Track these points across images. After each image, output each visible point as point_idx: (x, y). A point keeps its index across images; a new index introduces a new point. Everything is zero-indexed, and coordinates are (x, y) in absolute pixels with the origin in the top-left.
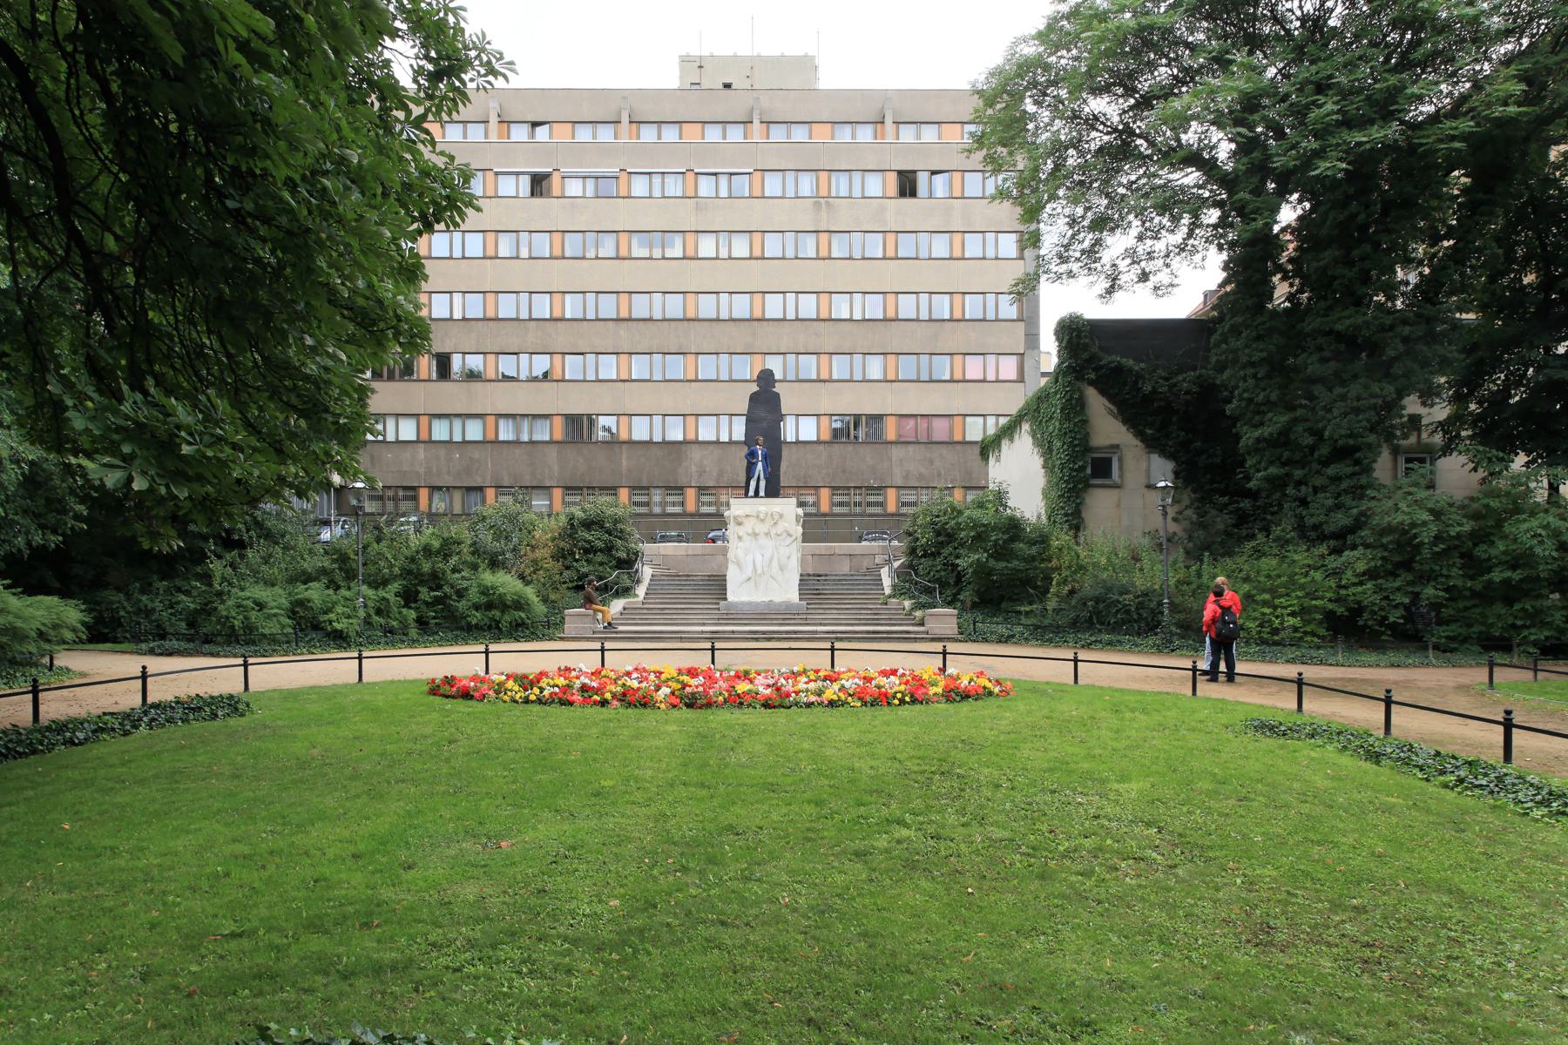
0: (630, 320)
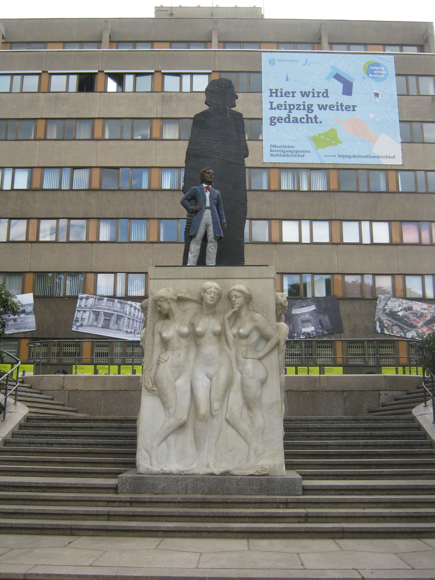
0: (101, 190)
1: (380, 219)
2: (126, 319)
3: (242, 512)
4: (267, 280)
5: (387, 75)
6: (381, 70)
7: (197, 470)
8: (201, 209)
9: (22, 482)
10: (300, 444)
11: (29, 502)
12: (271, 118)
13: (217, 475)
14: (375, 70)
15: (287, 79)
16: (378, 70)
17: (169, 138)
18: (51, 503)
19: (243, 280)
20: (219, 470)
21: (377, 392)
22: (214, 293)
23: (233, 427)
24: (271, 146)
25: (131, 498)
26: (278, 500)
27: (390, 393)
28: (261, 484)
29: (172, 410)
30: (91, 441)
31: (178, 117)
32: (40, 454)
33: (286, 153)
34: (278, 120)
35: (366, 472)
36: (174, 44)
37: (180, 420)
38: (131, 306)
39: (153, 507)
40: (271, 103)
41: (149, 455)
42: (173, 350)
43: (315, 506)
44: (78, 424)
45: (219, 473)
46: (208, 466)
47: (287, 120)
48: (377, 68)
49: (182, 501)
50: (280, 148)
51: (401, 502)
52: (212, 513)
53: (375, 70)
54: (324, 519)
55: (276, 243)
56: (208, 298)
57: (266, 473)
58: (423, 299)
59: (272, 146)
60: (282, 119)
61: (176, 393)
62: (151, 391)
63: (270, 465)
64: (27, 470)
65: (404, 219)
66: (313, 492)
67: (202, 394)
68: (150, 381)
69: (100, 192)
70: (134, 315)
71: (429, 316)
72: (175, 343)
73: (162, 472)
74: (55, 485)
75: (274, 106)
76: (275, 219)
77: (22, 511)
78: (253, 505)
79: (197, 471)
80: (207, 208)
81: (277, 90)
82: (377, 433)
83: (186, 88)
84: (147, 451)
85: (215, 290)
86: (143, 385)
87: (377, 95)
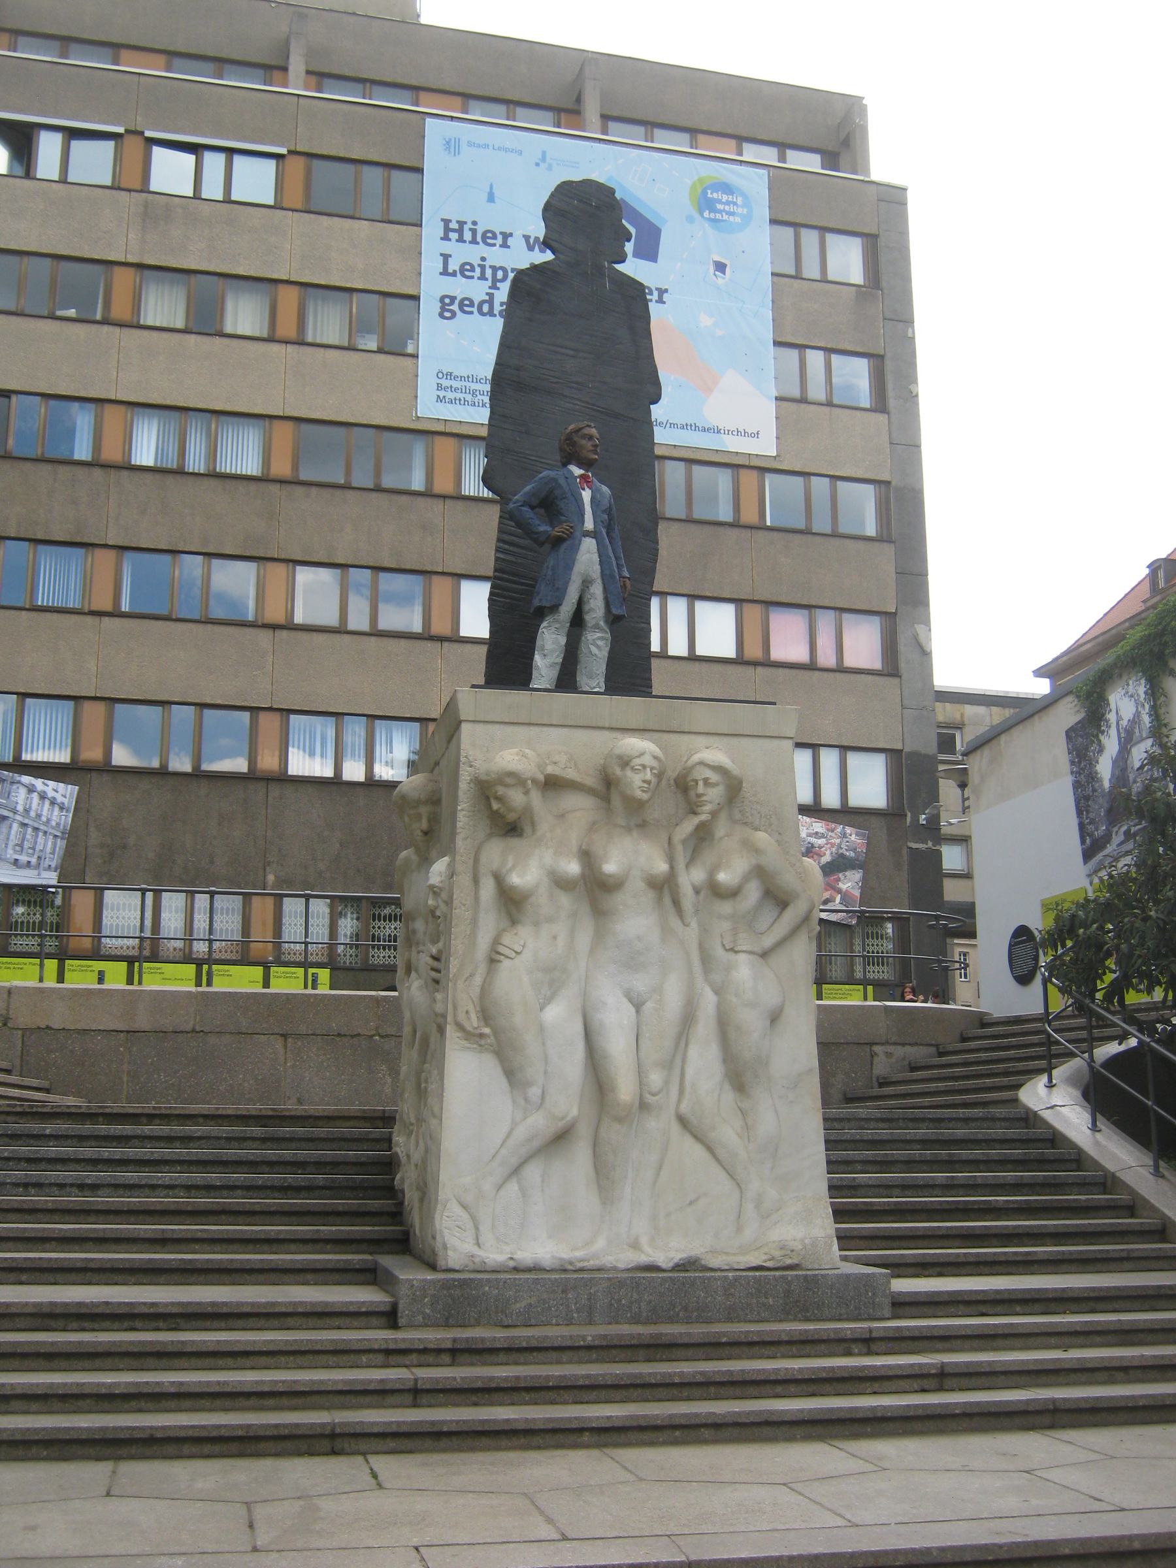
1: (715, 595)
2: (15, 826)
3: (779, 1370)
4: (776, 742)
5: (747, 219)
6: (735, 204)
7: (610, 1258)
8: (570, 535)
9: (107, 1303)
11: (151, 1362)
12: (442, 299)
13: (664, 1271)
14: (720, 202)
15: (491, 198)
16: (728, 203)
17: (158, 324)
18: (221, 1362)
19: (716, 738)
20: (672, 1254)
21: (867, 1048)
22: (652, 769)
23: (697, 1138)
24: (440, 375)
25: (455, 1340)
26: (849, 1335)
27: (899, 1051)
28: (788, 1293)
29: (534, 1092)
30: (214, 1177)
31: (185, 267)
32: (72, 1218)
33: (479, 397)
34: (461, 306)
35: (995, 1254)
36: (177, 62)
37: (563, 1118)
38: (31, 789)
39: (517, 1363)
40: (446, 257)
41: (473, 1218)
42: (536, 924)
43: (939, 1345)
44: (147, 1129)
45: (671, 1264)
46: (635, 1246)
47: (486, 308)
48: (725, 198)
49: (596, 1343)
50: (464, 383)
51: (1142, 1331)
52: (702, 1373)
53: (720, 202)
54: (983, 1381)
55: (441, 639)
56: (636, 782)
57: (795, 1261)
58: (814, 810)
59: (440, 374)
60: (472, 304)
61: (544, 1044)
62: (473, 1037)
63: (802, 1240)
64: (66, 1265)
65: (775, 599)
66: (913, 1310)
67: (618, 1045)
68: (471, 1007)
70: (39, 816)
71: (828, 853)
72: (542, 901)
73: (512, 1264)
74: (210, 1310)
75: (453, 266)
76: (443, 573)
77: (157, 1390)
78: (782, 1349)
79: (608, 1260)
80: (587, 534)
81: (462, 224)
82: (965, 1153)
83: (213, 189)
84: (464, 1207)
85: (654, 763)
86: (450, 1019)
87: (720, 267)
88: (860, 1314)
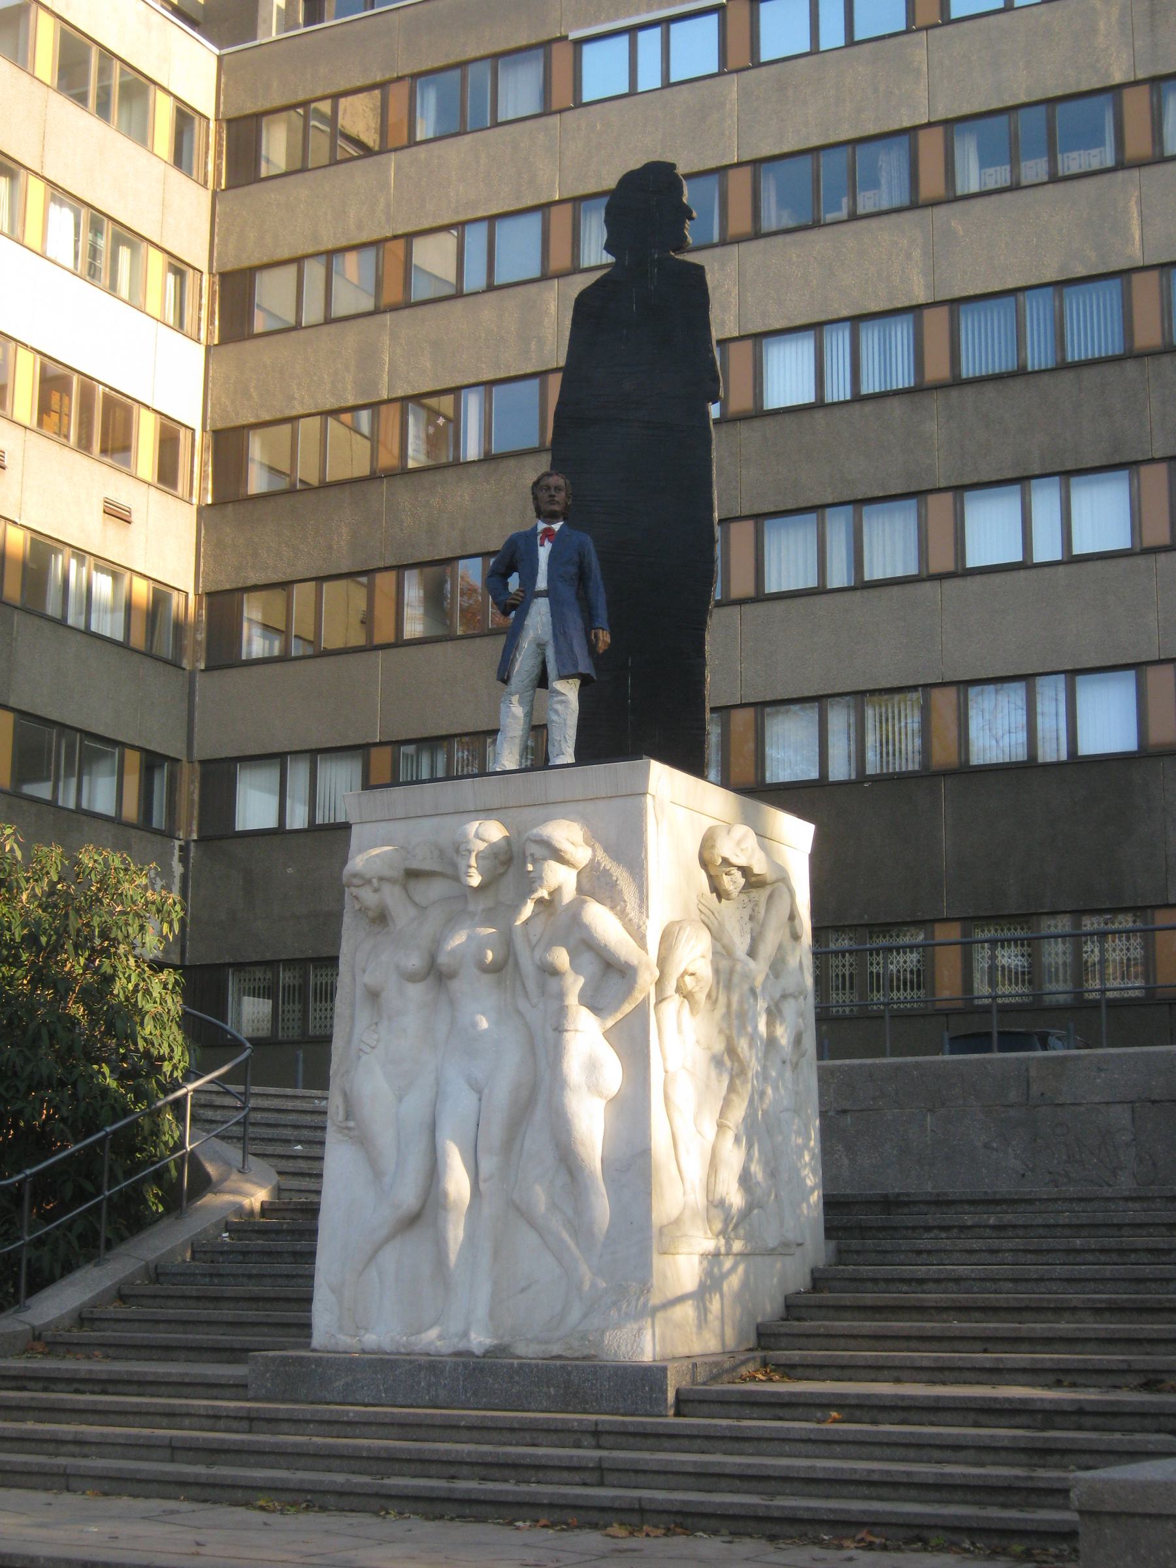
10: (878, 1276)
13: (478, 1357)
49: (357, 1419)
69: (954, 393)
80: (541, 594)
88: (637, 1410)
